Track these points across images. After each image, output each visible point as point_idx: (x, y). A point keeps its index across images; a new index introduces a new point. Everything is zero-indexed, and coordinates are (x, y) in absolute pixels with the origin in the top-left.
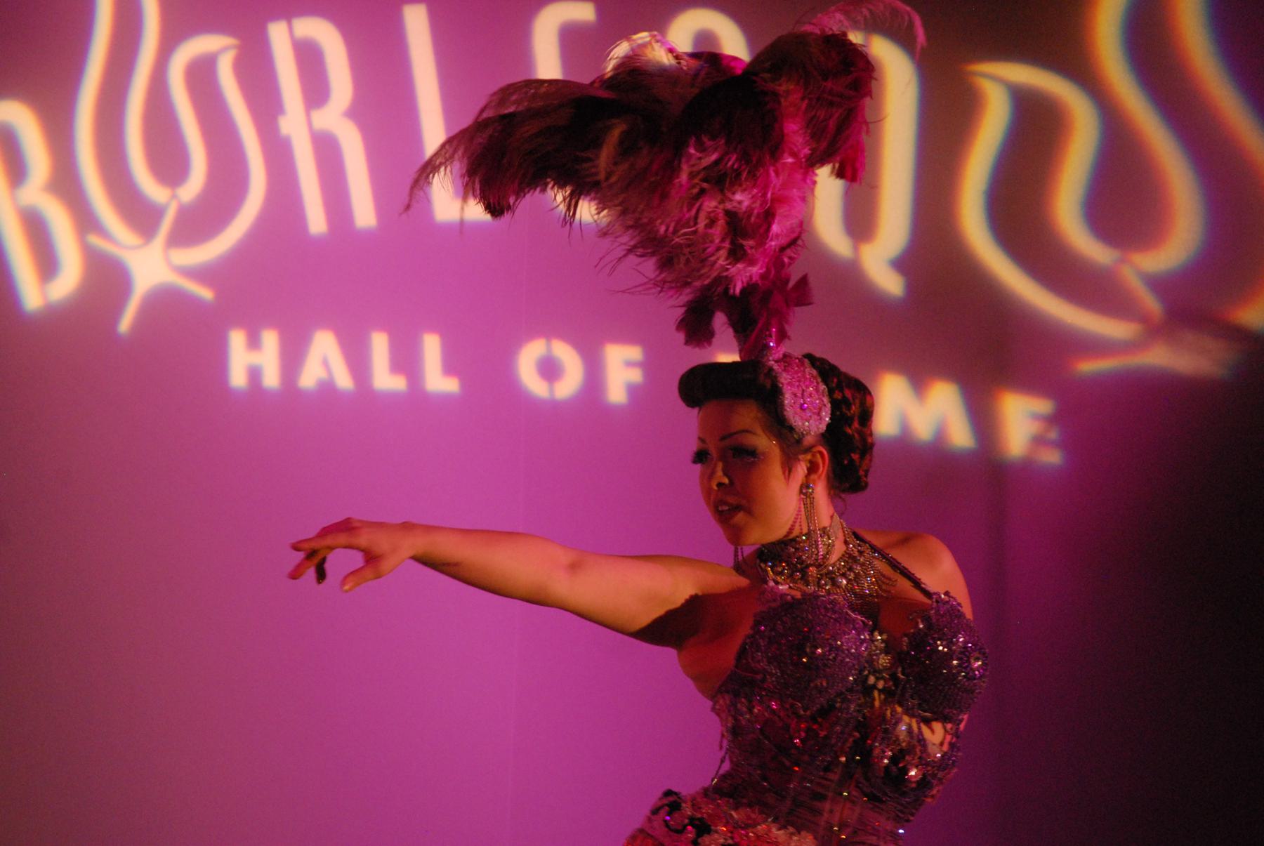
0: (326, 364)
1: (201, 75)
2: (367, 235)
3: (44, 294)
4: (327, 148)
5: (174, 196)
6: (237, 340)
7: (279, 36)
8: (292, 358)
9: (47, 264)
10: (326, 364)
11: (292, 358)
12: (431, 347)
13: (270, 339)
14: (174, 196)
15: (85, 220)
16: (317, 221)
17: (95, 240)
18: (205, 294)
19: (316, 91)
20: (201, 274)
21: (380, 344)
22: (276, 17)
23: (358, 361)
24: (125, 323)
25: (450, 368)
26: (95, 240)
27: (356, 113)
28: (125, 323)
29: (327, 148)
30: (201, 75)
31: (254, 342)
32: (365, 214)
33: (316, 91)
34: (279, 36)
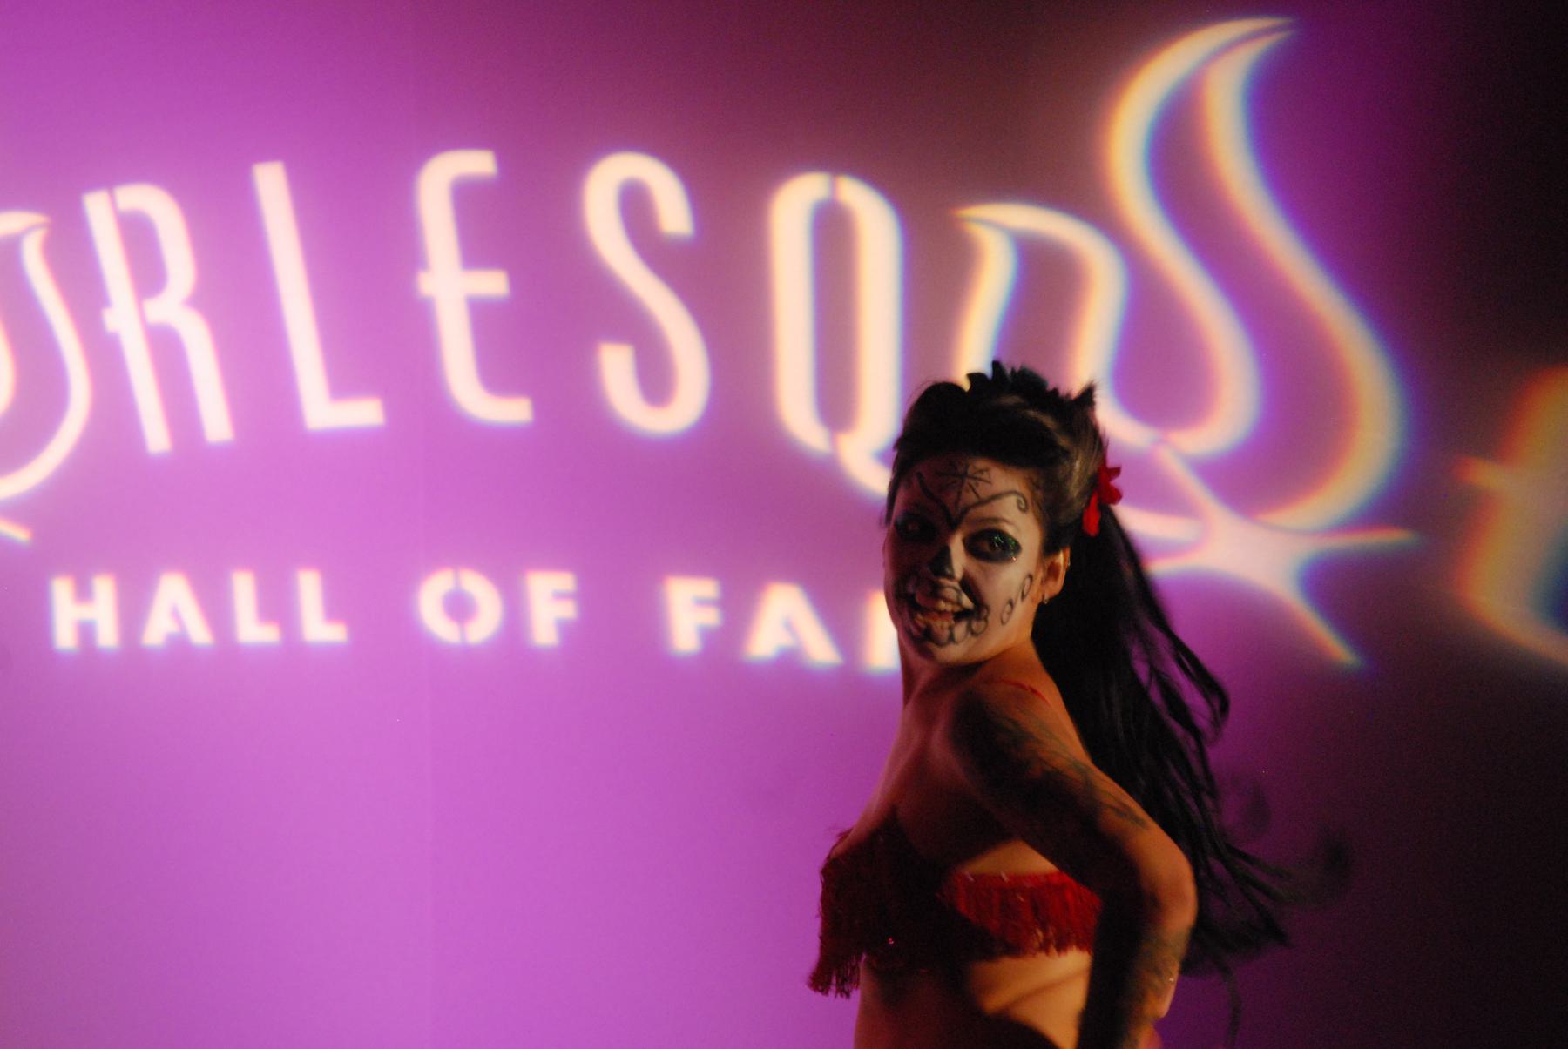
0: (176, 615)
2: (223, 453)
4: (166, 347)
6: (61, 591)
7: (99, 210)
8: (133, 611)
10: (176, 615)
11: (133, 611)
12: (309, 587)
13: (104, 588)
16: (157, 437)
19: (148, 277)
21: (244, 588)
23: (217, 609)
25: (334, 610)
27: (200, 300)
29: (166, 347)
31: (84, 593)
32: (217, 424)
33: (148, 277)
34: (99, 210)
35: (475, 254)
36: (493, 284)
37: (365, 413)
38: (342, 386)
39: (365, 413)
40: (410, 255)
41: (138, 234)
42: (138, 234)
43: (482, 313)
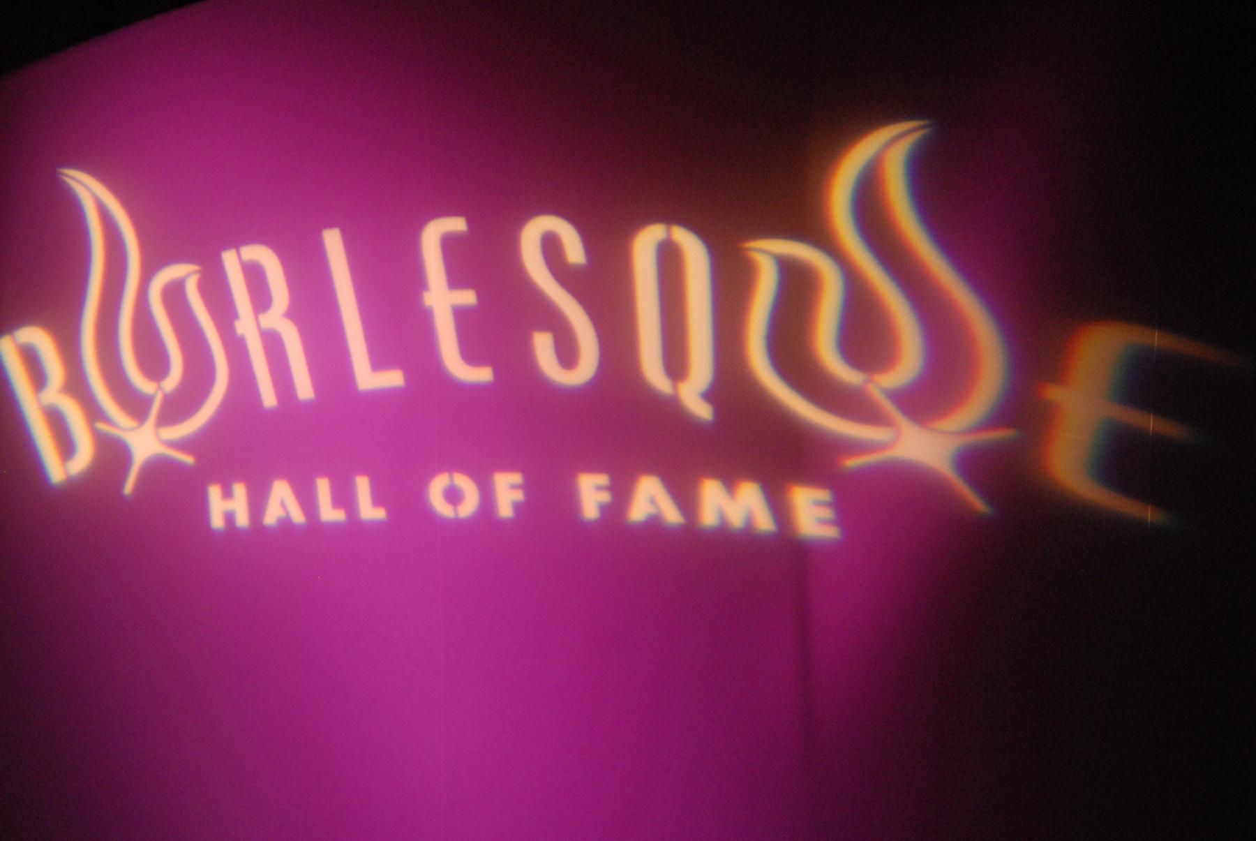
0: (283, 505)
1: (174, 294)
2: (308, 405)
4: (272, 342)
5: (159, 388)
6: (214, 492)
7: (230, 260)
8: (257, 504)
9: (66, 447)
10: (283, 505)
11: (257, 504)
12: (363, 486)
13: (240, 490)
14: (159, 388)
15: (93, 412)
16: (269, 398)
17: (101, 426)
18: (188, 460)
19: (261, 300)
20: (183, 445)
21: (323, 487)
23: (307, 500)
24: (129, 487)
25: (377, 501)
26: (101, 426)
27: (292, 314)
28: (129, 487)
29: (272, 342)
30: (174, 294)
31: (227, 494)
32: (304, 389)
33: (261, 300)
34: (230, 260)
35: (456, 280)
36: (468, 298)
37: (393, 379)
38: (379, 362)
39: (393, 379)
40: (418, 282)
41: (254, 275)
42: (254, 275)
43: (461, 316)
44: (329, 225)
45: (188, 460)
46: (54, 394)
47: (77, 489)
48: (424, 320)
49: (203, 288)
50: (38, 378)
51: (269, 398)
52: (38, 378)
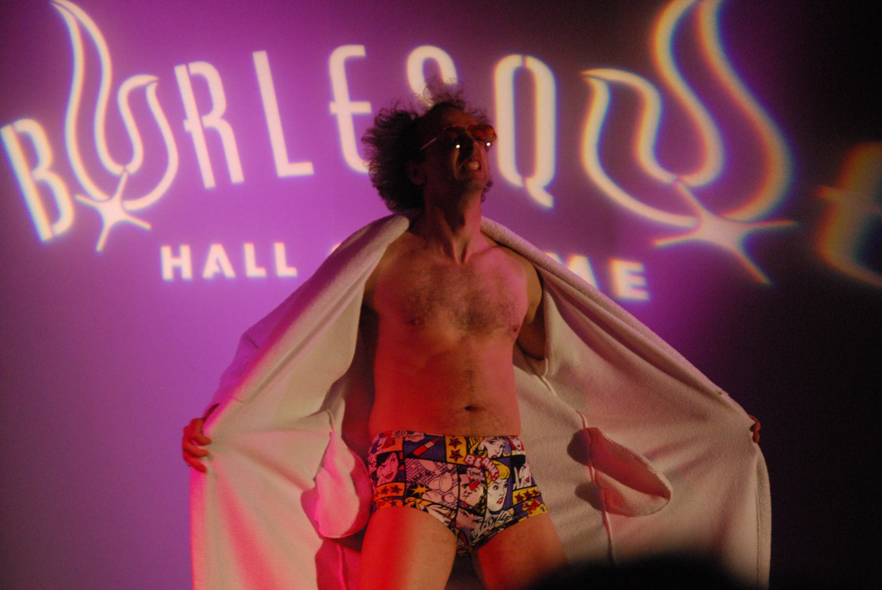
0: (218, 263)
1: (138, 99)
2: (238, 187)
3: (52, 230)
4: (213, 139)
5: (125, 170)
6: (166, 252)
7: (181, 73)
8: (198, 262)
9: (53, 213)
10: (218, 263)
11: (198, 262)
12: (280, 250)
13: (185, 251)
14: (125, 170)
15: (74, 187)
16: (209, 180)
17: (80, 198)
18: (146, 226)
19: (205, 105)
20: (142, 214)
21: (249, 251)
22: (179, 63)
23: (237, 261)
24: (100, 246)
25: (290, 262)
26: (80, 198)
27: (228, 116)
28: (100, 246)
29: (213, 139)
30: (138, 99)
31: (176, 253)
32: (237, 174)
33: (205, 105)
34: (181, 73)
35: (355, 94)
36: (364, 108)
37: (305, 169)
38: (294, 156)
39: (305, 169)
40: (327, 95)
41: (200, 85)
42: (200, 85)
43: (357, 120)
44: (259, 48)
45: (146, 226)
46: (44, 171)
47: (62, 244)
48: (331, 123)
49: (159, 94)
50: (32, 159)
51: (209, 180)
52: (32, 159)
